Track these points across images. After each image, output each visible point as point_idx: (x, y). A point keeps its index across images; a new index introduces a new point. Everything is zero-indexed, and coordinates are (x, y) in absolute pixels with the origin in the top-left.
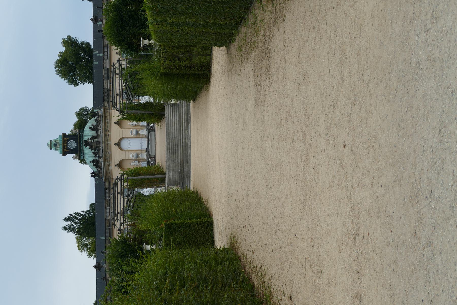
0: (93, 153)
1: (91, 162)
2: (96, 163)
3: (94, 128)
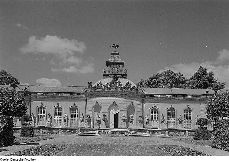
0: (108, 84)
1: (100, 82)
2: (100, 86)
3: (128, 85)
